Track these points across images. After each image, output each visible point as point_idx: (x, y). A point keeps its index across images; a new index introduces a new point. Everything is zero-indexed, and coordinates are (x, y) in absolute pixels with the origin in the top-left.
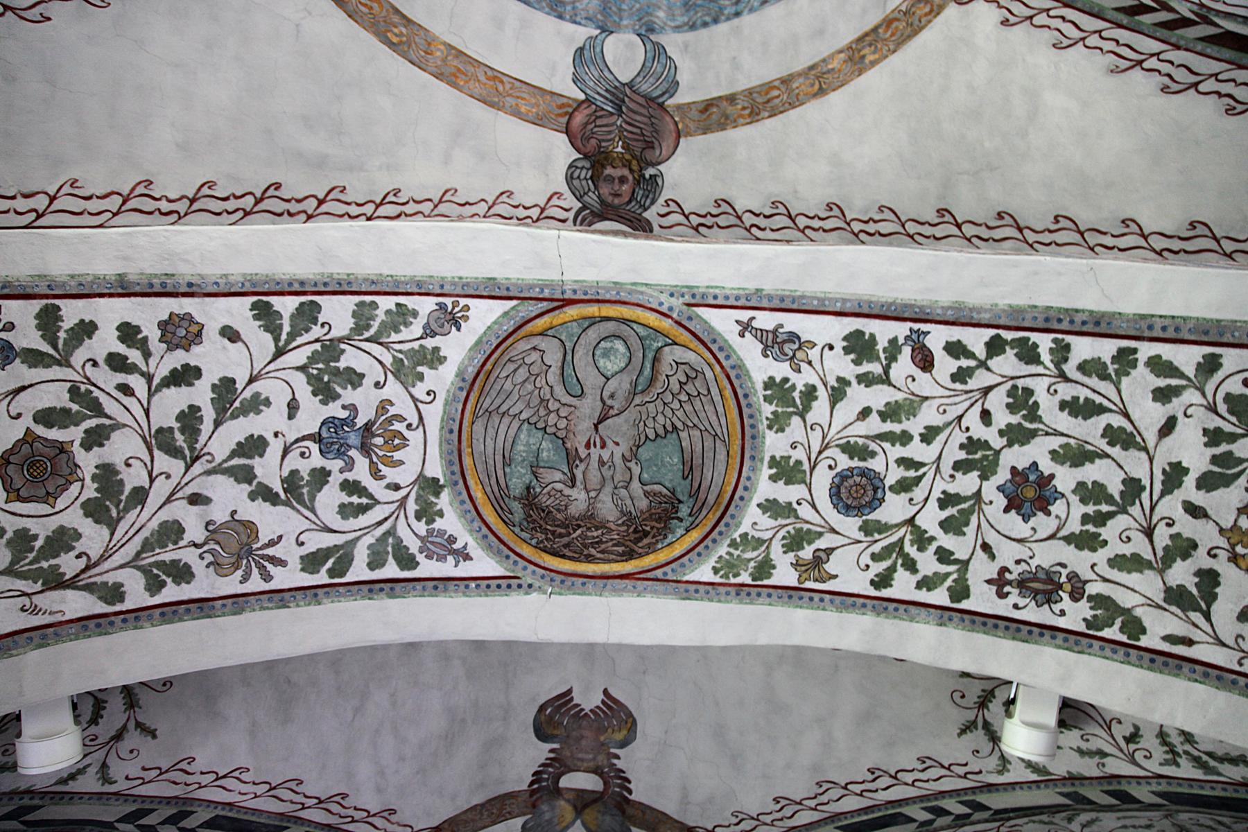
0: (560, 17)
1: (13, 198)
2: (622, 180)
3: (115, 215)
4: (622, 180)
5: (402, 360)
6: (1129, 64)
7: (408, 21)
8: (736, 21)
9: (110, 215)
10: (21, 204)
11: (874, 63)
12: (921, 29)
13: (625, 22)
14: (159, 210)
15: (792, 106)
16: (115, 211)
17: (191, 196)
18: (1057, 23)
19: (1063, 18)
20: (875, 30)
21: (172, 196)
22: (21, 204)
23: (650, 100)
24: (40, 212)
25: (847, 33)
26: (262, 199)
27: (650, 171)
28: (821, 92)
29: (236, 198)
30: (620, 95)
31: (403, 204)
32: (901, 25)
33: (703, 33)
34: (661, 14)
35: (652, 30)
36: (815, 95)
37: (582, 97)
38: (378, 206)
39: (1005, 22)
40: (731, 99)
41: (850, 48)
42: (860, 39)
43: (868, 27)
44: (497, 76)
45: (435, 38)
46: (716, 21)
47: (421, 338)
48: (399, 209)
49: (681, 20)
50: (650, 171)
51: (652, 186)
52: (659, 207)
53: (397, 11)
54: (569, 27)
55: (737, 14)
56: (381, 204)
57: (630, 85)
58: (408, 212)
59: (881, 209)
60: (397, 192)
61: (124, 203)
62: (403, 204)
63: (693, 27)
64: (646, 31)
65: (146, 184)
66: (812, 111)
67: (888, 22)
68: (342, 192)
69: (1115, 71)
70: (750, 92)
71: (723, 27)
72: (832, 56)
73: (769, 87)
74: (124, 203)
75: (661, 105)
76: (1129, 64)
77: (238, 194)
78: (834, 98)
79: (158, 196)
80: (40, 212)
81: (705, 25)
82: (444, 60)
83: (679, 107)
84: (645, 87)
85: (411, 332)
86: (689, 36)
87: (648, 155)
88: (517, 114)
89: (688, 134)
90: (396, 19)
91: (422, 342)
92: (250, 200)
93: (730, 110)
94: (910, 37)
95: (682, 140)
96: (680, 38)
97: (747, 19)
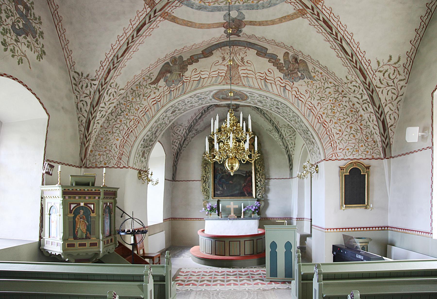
0: (220, 11)
2: (235, 30)
4: (235, 30)
6: (327, 40)
7: (191, 22)
8: (257, 10)
10: (146, 70)
11: (284, 22)
12: (294, 19)
13: (234, 9)
15: (267, 25)
18: (319, 29)
19: (320, 28)
20: (285, 16)
22: (146, 70)
23: (239, 20)
25: (280, 16)
27: (240, 29)
28: (273, 24)
30: (233, 20)
32: (291, 17)
33: (251, 11)
34: (241, 7)
35: (239, 10)
36: (272, 24)
37: (226, 21)
39: (310, 24)
40: (256, 22)
41: (280, 18)
42: (282, 18)
43: (284, 16)
44: (209, 24)
45: (197, 23)
46: (253, 9)
49: (245, 8)
50: (240, 29)
51: (241, 31)
52: (242, 33)
53: (188, 21)
54: (222, 12)
55: (257, 9)
57: (236, 18)
59: (281, 42)
63: (248, 9)
64: (238, 9)
66: (271, 27)
67: (288, 16)
69: (325, 40)
70: (259, 22)
71: (254, 11)
72: (276, 19)
73: (263, 21)
75: (242, 21)
76: (327, 40)
78: (275, 25)
81: (251, 9)
82: (199, 26)
83: (245, 21)
84: (238, 18)
86: (248, 11)
87: (239, 27)
88: (214, 28)
89: (247, 25)
90: (189, 22)
93: (255, 23)
94: (292, 20)
95: (246, 26)
96: (245, 11)
97: (259, 10)
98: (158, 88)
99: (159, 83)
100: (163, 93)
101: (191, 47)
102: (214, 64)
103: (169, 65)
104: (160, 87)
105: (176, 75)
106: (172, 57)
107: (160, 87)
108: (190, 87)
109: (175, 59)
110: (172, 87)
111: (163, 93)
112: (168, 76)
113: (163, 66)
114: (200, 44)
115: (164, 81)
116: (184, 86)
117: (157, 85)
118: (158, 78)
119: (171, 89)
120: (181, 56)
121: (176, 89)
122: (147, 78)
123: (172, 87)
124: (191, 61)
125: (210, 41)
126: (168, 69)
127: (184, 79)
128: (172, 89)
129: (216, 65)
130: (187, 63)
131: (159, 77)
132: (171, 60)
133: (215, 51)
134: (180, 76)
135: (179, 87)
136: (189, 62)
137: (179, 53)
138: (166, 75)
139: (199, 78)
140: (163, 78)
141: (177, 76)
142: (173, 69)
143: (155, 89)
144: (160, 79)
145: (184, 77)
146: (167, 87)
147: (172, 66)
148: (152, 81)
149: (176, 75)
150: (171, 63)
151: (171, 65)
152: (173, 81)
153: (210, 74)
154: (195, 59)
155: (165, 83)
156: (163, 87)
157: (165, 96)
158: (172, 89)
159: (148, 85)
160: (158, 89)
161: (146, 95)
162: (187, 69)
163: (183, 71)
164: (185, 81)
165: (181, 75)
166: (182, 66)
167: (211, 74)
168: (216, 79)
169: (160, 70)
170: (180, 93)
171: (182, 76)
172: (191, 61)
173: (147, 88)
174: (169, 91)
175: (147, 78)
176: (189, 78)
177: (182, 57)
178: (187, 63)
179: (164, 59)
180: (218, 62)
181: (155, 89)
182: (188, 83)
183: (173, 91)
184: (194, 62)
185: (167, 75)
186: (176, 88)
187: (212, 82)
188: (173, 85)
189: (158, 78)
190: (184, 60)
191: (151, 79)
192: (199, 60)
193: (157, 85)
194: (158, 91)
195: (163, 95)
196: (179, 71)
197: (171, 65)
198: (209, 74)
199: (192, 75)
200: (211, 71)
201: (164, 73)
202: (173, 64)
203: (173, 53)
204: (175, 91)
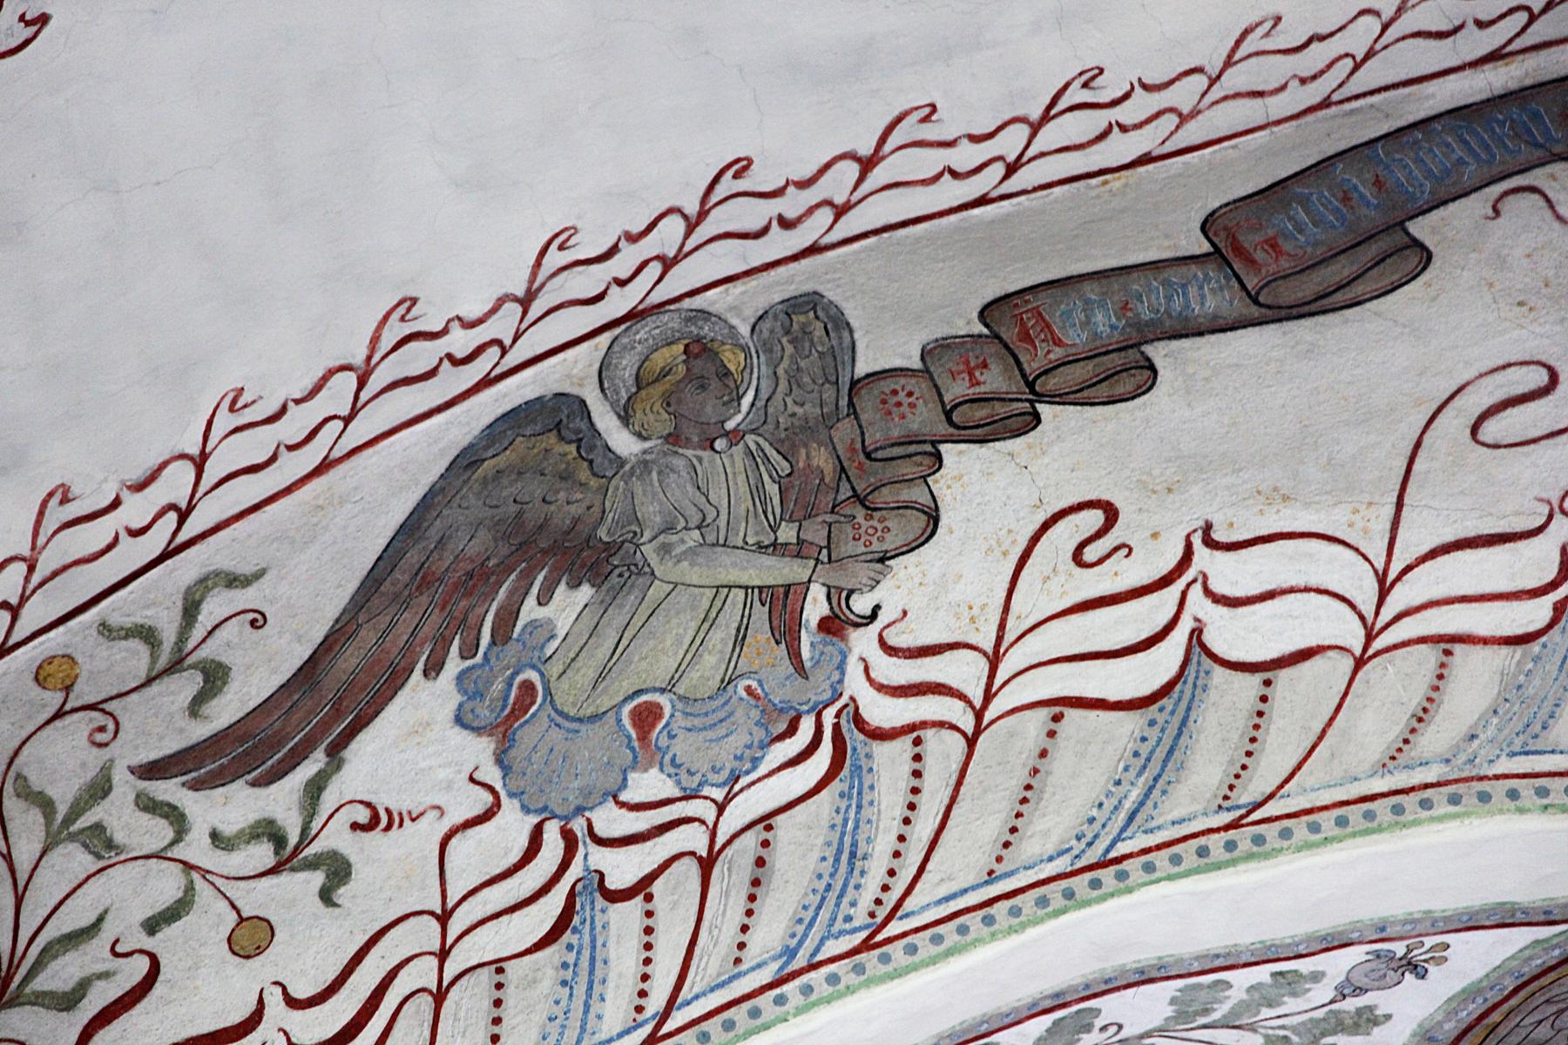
1: (116, 504)
3: (347, 420)
5: (1286, 1037)
9: (339, 424)
10: (136, 510)
14: (449, 356)
16: (345, 412)
17: (520, 291)
21: (473, 311)
22: (136, 510)
24: (183, 505)
26: (703, 214)
29: (633, 238)
31: (1115, 103)
38: (1036, 128)
47: (1332, 1002)
48: (1101, 119)
56: (1046, 117)
58: (1127, 120)
60: (1090, 78)
61: (362, 384)
62: (1115, 103)
65: (401, 310)
68: (926, 119)
74: (362, 384)
77: (636, 228)
79: (438, 328)
80: (183, 505)
85: (1309, 1000)
91: (1334, 1007)
92: (673, 228)
98: (335, 838)
99: (366, 750)
100: (426, 934)
101: (1011, 143)
102: (1455, 422)
103: (588, 439)
104: (374, 821)
105: (709, 621)
106: (633, 316)
107: (374, 821)
108: (992, 827)
109: (698, 350)
110: (611, 820)
111: (426, 934)
112: (543, 629)
113: (466, 461)
114: (1184, 95)
115: (459, 720)
116: (858, 798)
117: (315, 789)
118: (349, 660)
119: (601, 858)
120: (810, 302)
121: (707, 865)
122: (133, 659)
123: (611, 820)
124: (995, 379)
125: (1362, 35)
126: (567, 507)
127: (855, 684)
128: (623, 868)
129: (1493, 430)
130: (924, 418)
131: (368, 635)
132: (627, 367)
133: (1477, 204)
134: (787, 632)
135: (765, 821)
136: (956, 390)
137: (780, 244)
138: (508, 617)
139: (1164, 661)
140: (454, 665)
141: (721, 636)
142: (651, 511)
143: (263, 854)
144: (395, 681)
145: (863, 642)
146: (512, 827)
147: (644, 465)
148: (226, 710)
149: (709, 621)
150: (625, 418)
151: (623, 442)
152: (646, 717)
153: (1384, 593)
154: (1076, 338)
155: (479, 751)
156: (430, 831)
157: (469, 1001)
158: (623, 868)
159: (125, 787)
160: (338, 871)
161: (62, 974)
162: (933, 518)
163: (848, 547)
164: (883, 711)
165: (816, 607)
166: (822, 459)
167: (1399, 599)
168: (1512, 689)
169: (410, 529)
170: (769, 934)
171: (833, 626)
172: (995, 379)
173: (100, 842)
174: (554, 903)
175: (133, 659)
176: (965, 671)
177: (838, 323)
178: (924, 418)
179: (501, 326)
180: (1539, 377)
181: (263, 854)
182: (944, 750)
183: (642, 887)
184: (1059, 398)
185: (530, 610)
186: (693, 839)
187: (1436, 738)
188: (649, 784)
189: (349, 660)
190: (862, 369)
191: (215, 677)
192: (1158, 353)
193: (315, 789)
194: (326, 896)
195: (422, 974)
196: (776, 548)
197: (623, 442)
198: (1366, 595)
199: (1028, 605)
200: (1413, 542)
201: (480, 579)
202: (662, 423)
203: (670, 234)
204: (680, 885)
